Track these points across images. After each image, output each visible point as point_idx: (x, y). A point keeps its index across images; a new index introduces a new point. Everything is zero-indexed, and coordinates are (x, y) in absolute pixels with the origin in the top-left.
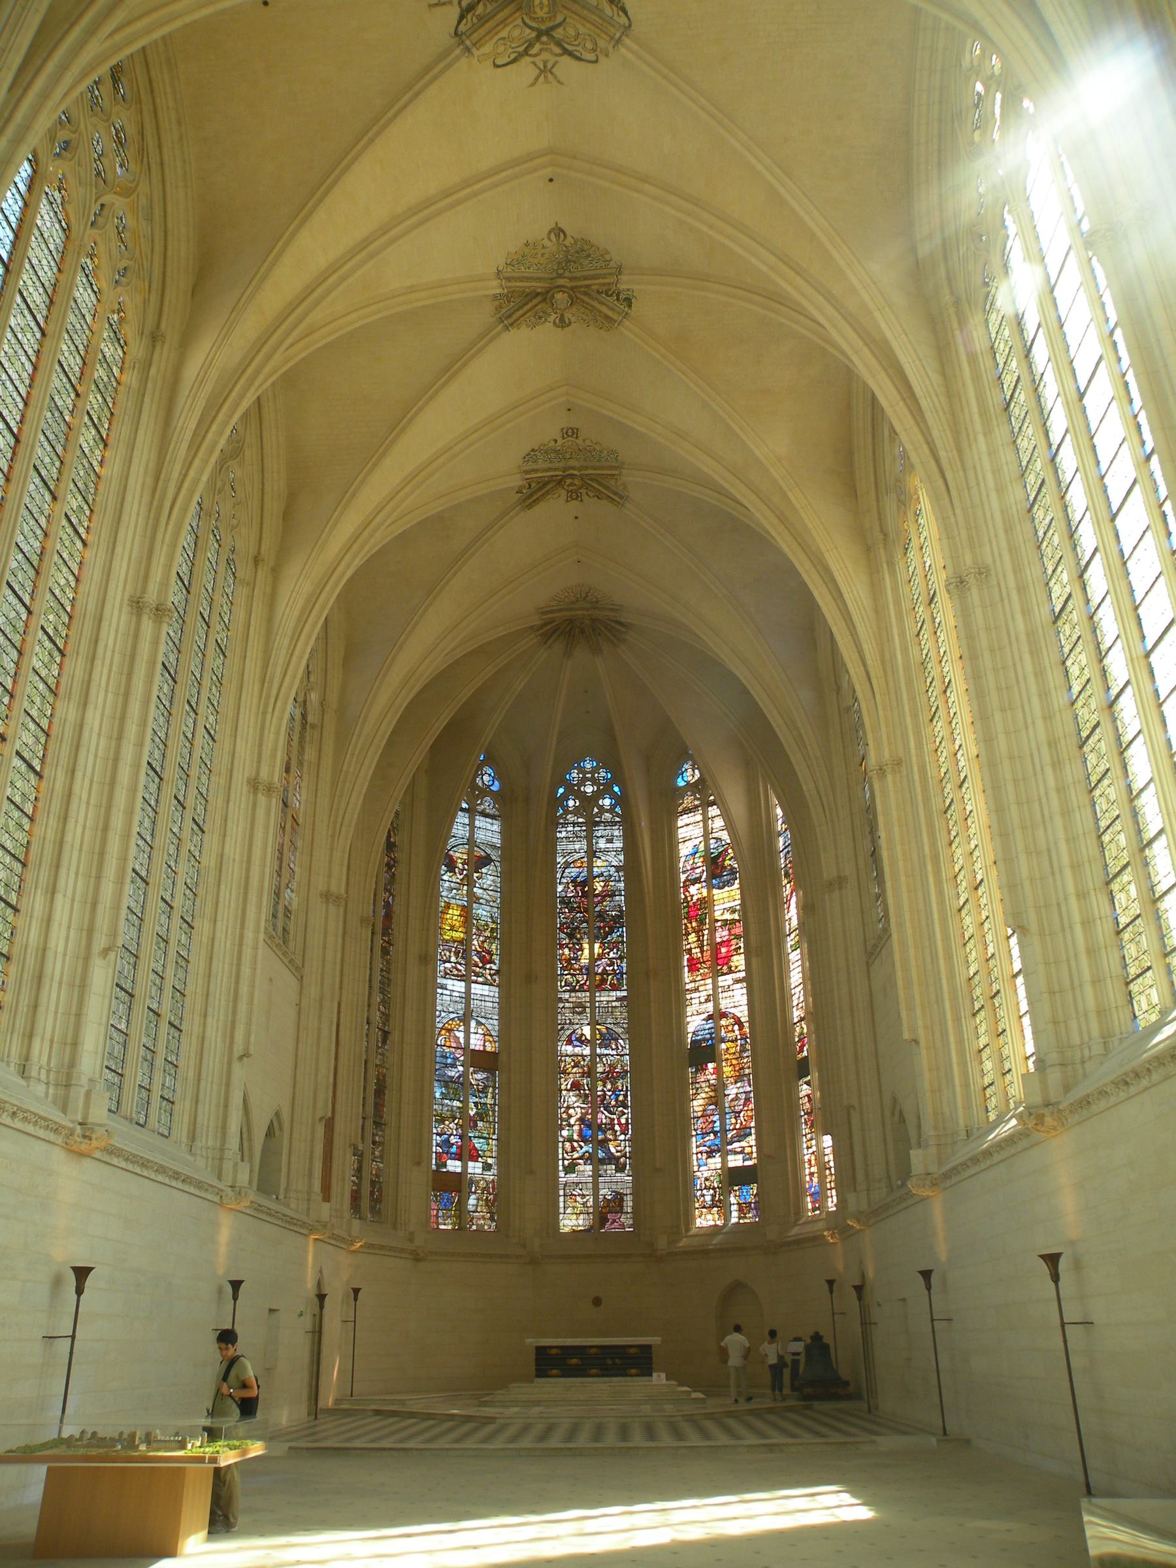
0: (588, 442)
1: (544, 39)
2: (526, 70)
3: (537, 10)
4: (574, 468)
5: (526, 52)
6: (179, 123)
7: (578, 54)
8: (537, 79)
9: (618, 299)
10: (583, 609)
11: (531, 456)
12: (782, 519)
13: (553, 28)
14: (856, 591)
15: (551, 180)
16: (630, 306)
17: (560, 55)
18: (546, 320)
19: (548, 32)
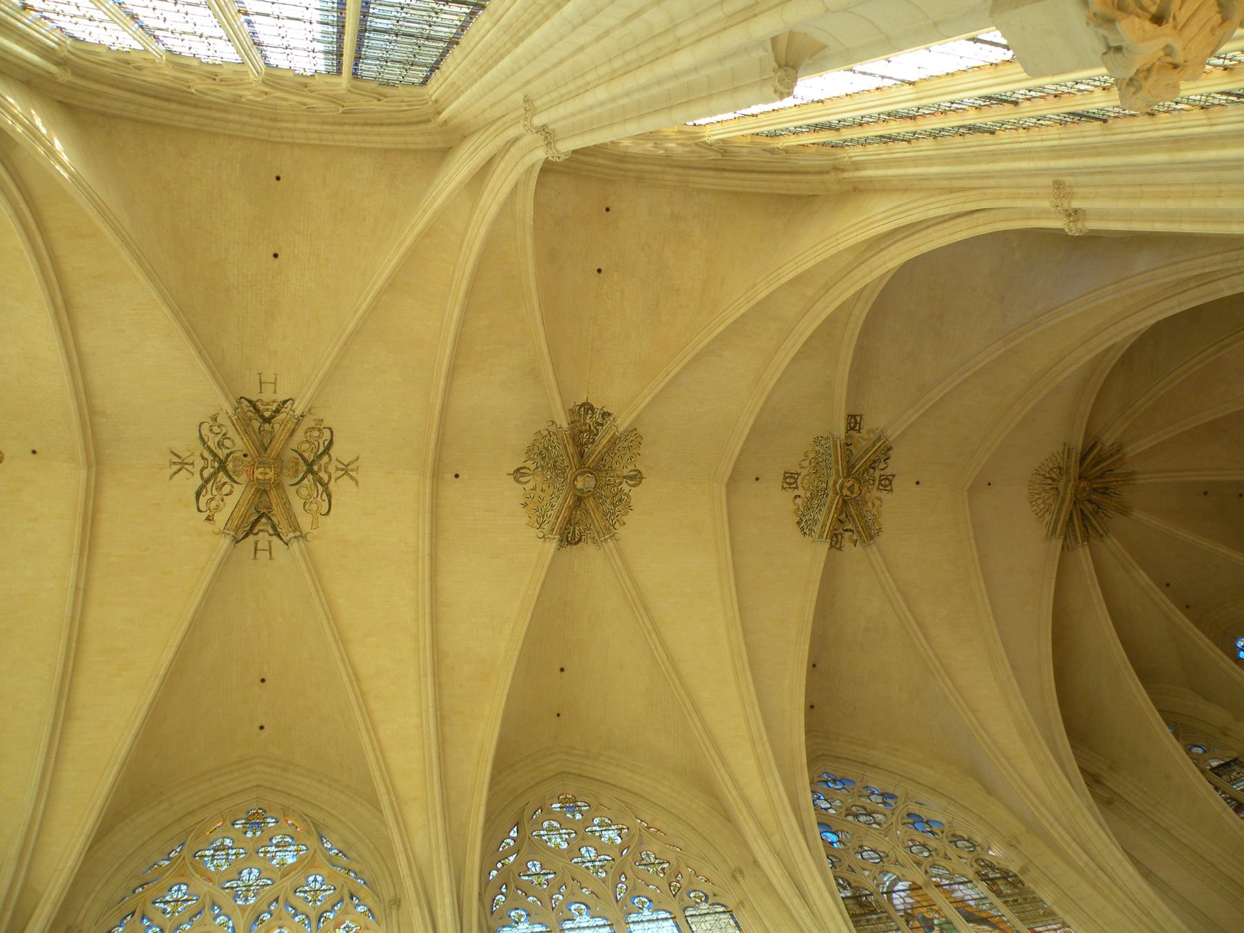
0: (806, 464)
1: (316, 468)
2: (341, 489)
3: (267, 477)
4: (835, 482)
5: (325, 485)
6: (320, 782)
9: (602, 425)
10: (1066, 487)
11: (804, 525)
12: (827, 289)
13: (305, 460)
14: (878, 216)
15: (457, 476)
16: (610, 414)
18: (628, 495)
19: (310, 465)
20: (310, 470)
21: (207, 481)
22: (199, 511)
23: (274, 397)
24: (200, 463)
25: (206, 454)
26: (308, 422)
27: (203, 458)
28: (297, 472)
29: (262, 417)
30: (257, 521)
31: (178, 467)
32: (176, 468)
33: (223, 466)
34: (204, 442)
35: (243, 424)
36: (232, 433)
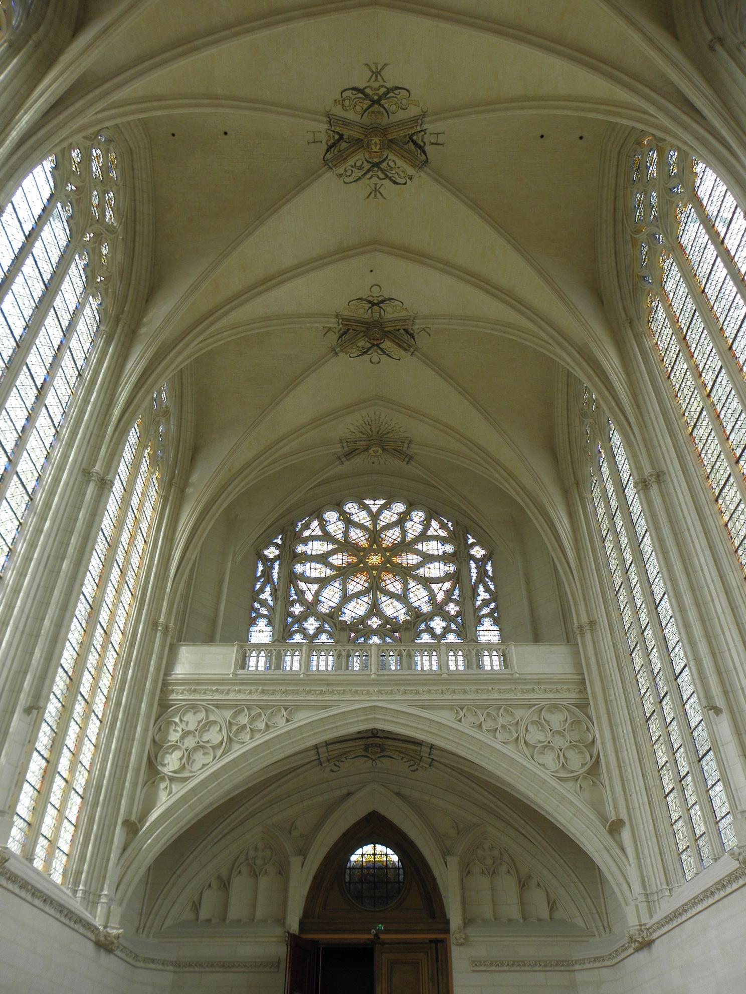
2: (391, 77)
3: (378, 142)
5: (389, 91)
7: (354, 92)
8: (383, 68)
13: (371, 106)
17: (366, 88)
19: (374, 102)
20: (378, 102)
21: (387, 176)
22: (405, 184)
23: (324, 132)
24: (375, 180)
25: (368, 176)
26: (338, 111)
27: (371, 177)
28: (379, 112)
29: (339, 140)
30: (415, 143)
31: (378, 194)
32: (378, 195)
33: (377, 165)
34: (360, 178)
35: (341, 158)
36: (351, 162)
